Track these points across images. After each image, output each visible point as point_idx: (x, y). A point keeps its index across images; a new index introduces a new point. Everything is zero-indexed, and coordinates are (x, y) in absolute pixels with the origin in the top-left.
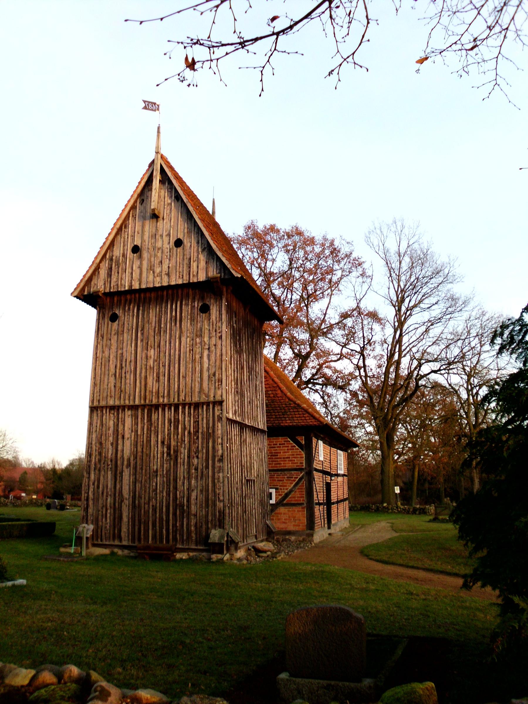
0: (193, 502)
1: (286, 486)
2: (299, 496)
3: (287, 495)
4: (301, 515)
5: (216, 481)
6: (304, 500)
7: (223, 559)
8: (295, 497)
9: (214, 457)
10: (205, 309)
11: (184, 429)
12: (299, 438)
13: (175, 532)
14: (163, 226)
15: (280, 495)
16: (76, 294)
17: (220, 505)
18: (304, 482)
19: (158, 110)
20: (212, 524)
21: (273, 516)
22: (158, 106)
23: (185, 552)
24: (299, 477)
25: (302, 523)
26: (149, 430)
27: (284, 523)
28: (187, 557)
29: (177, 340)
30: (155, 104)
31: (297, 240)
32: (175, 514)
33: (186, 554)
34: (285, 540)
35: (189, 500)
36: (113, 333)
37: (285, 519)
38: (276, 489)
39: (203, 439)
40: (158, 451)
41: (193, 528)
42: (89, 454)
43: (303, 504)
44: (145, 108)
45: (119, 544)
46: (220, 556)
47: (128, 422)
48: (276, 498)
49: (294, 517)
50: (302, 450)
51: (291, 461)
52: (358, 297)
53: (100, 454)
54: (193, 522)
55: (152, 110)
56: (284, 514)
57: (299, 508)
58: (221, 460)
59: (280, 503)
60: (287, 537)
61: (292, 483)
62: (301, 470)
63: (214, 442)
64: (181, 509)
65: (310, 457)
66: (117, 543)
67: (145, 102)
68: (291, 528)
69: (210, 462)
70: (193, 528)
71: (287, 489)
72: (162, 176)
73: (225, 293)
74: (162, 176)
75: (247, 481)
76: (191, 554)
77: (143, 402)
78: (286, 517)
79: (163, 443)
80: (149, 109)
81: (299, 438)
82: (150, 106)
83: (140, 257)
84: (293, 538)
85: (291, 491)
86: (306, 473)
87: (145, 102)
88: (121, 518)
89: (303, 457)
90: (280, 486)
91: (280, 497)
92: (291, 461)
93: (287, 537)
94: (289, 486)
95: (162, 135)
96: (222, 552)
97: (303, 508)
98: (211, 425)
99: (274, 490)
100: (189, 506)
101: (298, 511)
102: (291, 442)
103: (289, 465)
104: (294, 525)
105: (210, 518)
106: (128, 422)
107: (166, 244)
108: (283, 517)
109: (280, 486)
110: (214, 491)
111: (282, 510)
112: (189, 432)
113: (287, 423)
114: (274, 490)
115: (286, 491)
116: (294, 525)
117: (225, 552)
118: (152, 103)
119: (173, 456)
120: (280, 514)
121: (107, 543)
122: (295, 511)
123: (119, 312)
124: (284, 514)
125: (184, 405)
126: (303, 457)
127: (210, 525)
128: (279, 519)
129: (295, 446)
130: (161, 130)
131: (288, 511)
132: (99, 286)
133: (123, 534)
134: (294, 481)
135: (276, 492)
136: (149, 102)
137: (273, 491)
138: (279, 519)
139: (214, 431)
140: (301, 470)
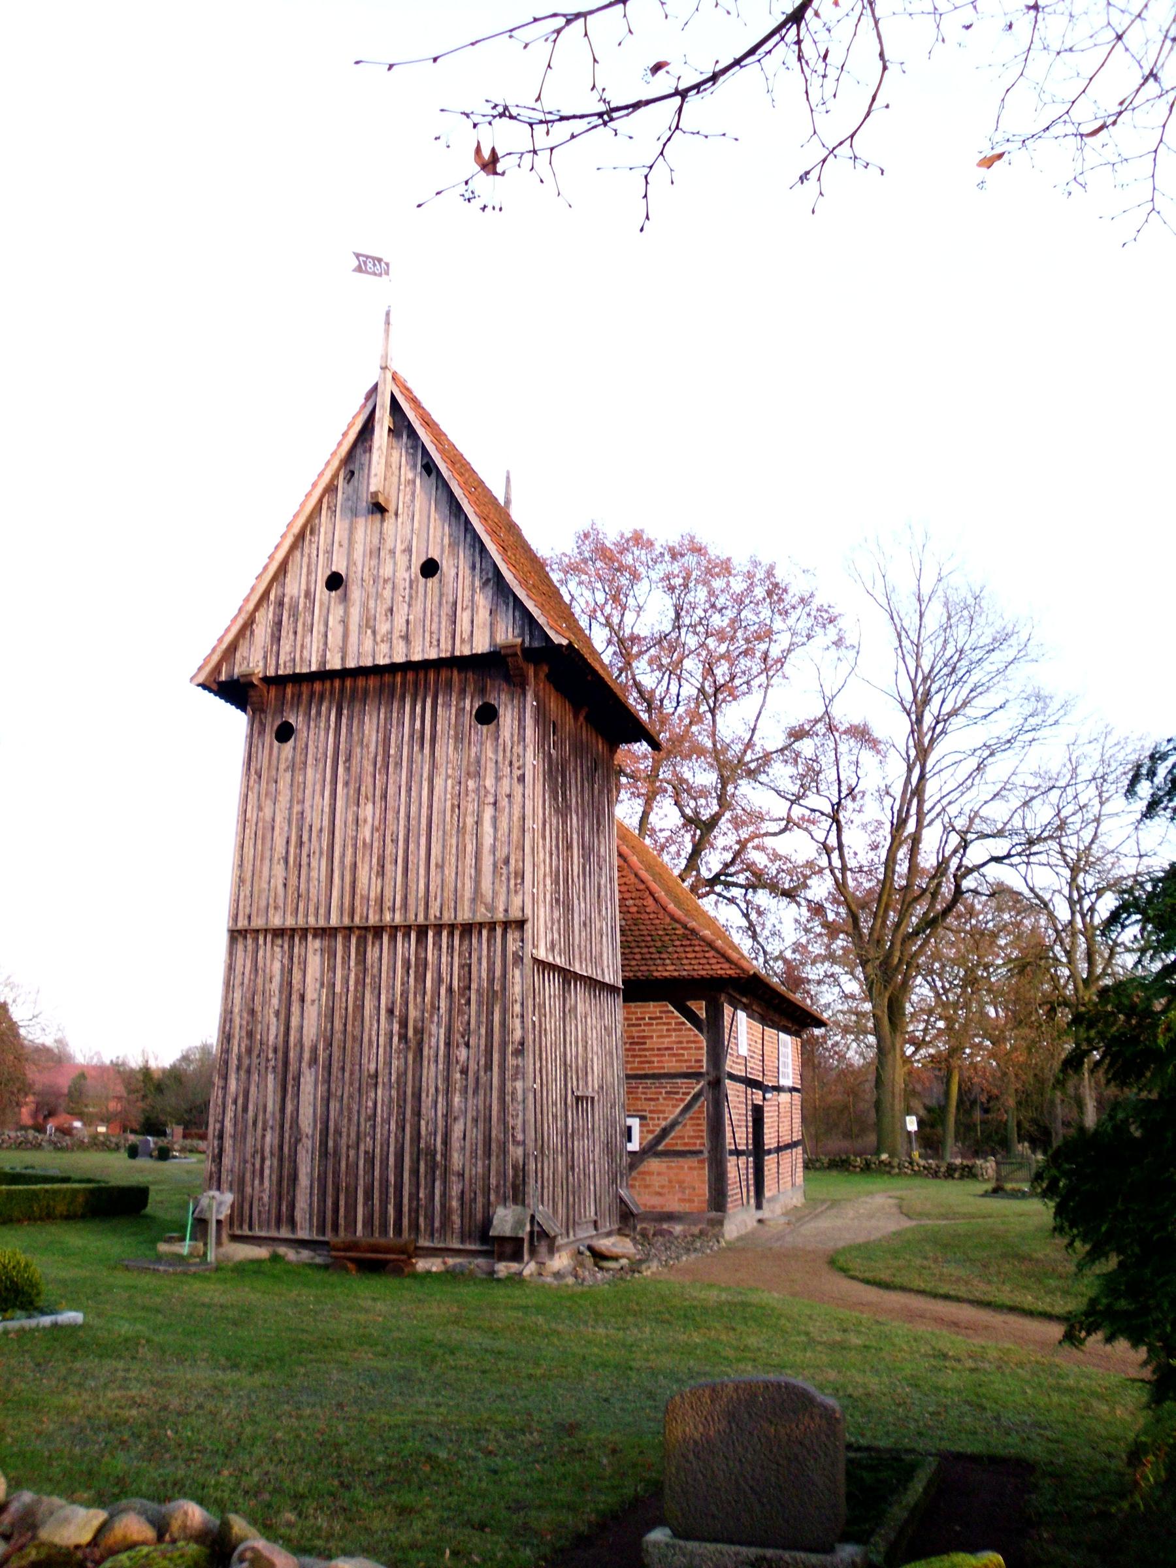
0: (456, 1144)
1: (663, 1112)
2: (692, 1133)
3: (665, 1132)
4: (697, 1177)
5: (508, 1098)
6: (703, 1143)
7: (520, 1274)
8: (682, 1138)
9: (504, 1044)
10: (487, 715)
11: (440, 980)
12: (693, 1005)
13: (414, 1212)
14: (395, 529)
15: (649, 1132)
16: (200, 679)
17: (516, 1152)
19: (387, 273)
20: (497, 1193)
21: (635, 1179)
22: (387, 264)
24: (693, 1092)
26: (361, 983)
27: (660, 1194)
28: (442, 1268)
30: (380, 260)
31: (692, 565)
32: (415, 1172)
33: (438, 1261)
34: (659, 1233)
36: (282, 766)
37: (663, 1187)
38: (642, 1118)
39: (479, 1003)
40: (379, 1029)
42: (226, 1037)
43: (701, 1152)
44: (359, 269)
45: (290, 1236)
46: (514, 1266)
47: (314, 963)
48: (641, 1138)
50: (701, 1030)
51: (675, 1055)
52: (828, 694)
53: (250, 1034)
54: (455, 1190)
56: (659, 1174)
57: (692, 1161)
58: (520, 1052)
59: (649, 1150)
60: (665, 1226)
61: (676, 1106)
62: (697, 1076)
63: (504, 1011)
64: (430, 1162)
65: (717, 1051)
66: (284, 1233)
67: (358, 256)
68: (673, 1204)
69: (496, 1056)
70: (455, 1204)
71: (665, 1119)
73: (532, 680)
74: (397, 419)
75: (578, 1098)
76: (451, 1261)
77: (346, 921)
78: (664, 1180)
79: (390, 1012)
80: (366, 272)
81: (693, 1005)
82: (369, 264)
83: (345, 598)
84: (678, 1229)
86: (709, 1083)
87: (358, 256)
88: (294, 1178)
90: (651, 1112)
91: (650, 1137)
92: (675, 1055)
93: (665, 1226)
94: (671, 1112)
96: (517, 1257)
98: (498, 973)
100: (446, 1155)
101: (690, 1168)
102: (677, 1013)
103: (671, 1065)
104: (682, 1200)
105: (493, 1181)
107: (404, 570)
108: (656, 1182)
109: (651, 1112)
112: (450, 990)
113: (667, 970)
114: (637, 1120)
115: (664, 1124)
117: (526, 1257)
118: (374, 258)
119: (412, 1040)
120: (650, 1174)
121: (263, 1234)
122: (682, 1168)
124: (659, 1174)
125: (439, 928)
126: (701, 1048)
127: (492, 1198)
129: (683, 1023)
131: (668, 1168)
132: (254, 662)
133: (298, 1215)
134: (682, 1100)
135: (641, 1125)
136: (367, 257)
137: (635, 1123)
138: (646, 1186)
139: (504, 988)
140: (697, 1076)
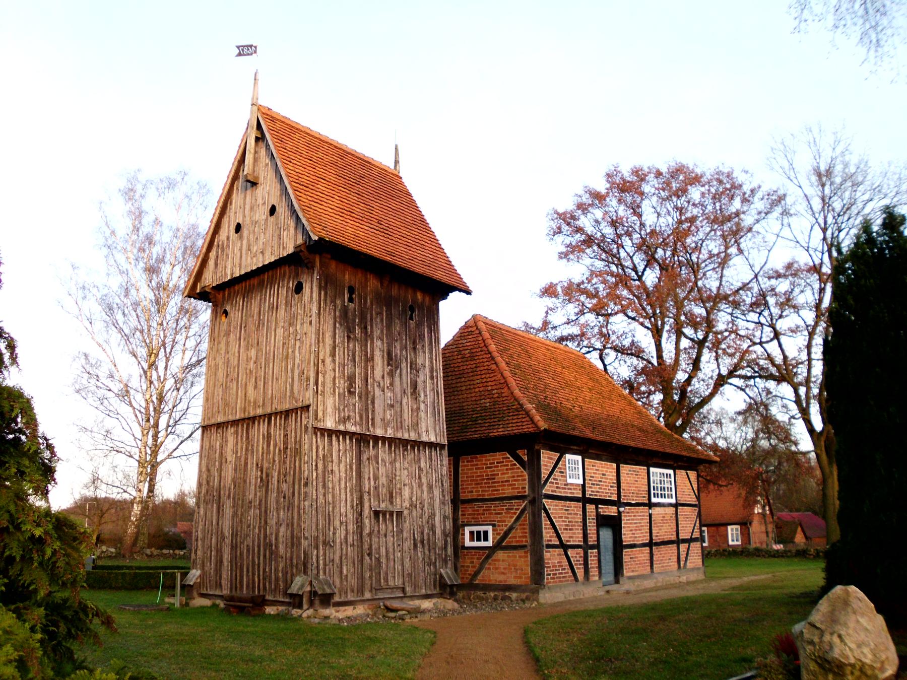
0: (281, 540)
1: (504, 521)
2: (521, 535)
3: (506, 534)
4: (523, 562)
5: (302, 511)
6: (527, 540)
7: (300, 616)
8: (515, 537)
9: (300, 480)
10: (299, 289)
11: (275, 445)
12: (520, 453)
13: (264, 579)
14: (260, 191)
15: (498, 534)
16: (186, 294)
17: (304, 543)
18: (527, 515)
19: (255, 52)
20: (297, 568)
21: (490, 564)
22: (256, 47)
23: (275, 606)
24: (521, 508)
25: (525, 574)
26: (247, 449)
27: (503, 573)
28: (276, 612)
29: (273, 333)
30: (251, 46)
31: (679, 181)
32: (265, 556)
33: (275, 608)
34: (504, 598)
35: (276, 539)
36: (222, 334)
37: (505, 569)
38: (494, 525)
39: (291, 457)
40: (253, 474)
41: (280, 575)
42: (200, 485)
43: (525, 546)
44: (239, 55)
45: (220, 594)
46: (300, 612)
47: (231, 440)
48: (493, 538)
49: (515, 566)
50: (525, 469)
51: (511, 485)
52: (806, 245)
53: (208, 482)
54: (281, 565)
55: (248, 54)
56: (503, 561)
57: (521, 552)
58: (306, 484)
59: (498, 546)
60: (507, 594)
61: (512, 517)
62: (523, 497)
63: (300, 460)
64: (270, 549)
65: (536, 481)
66: (218, 593)
67: (238, 47)
68: (512, 581)
69: (297, 487)
70: (280, 575)
71: (506, 526)
72: (268, 130)
73: (318, 264)
74: (268, 130)
75: (377, 514)
76: (280, 608)
77: (243, 416)
78: (505, 565)
79: (257, 465)
80: (244, 55)
81: (520, 453)
82: (246, 50)
83: (241, 238)
84: (514, 595)
85: (511, 529)
86: (530, 502)
87: (238, 47)
88: (221, 562)
89: (525, 480)
90: (499, 521)
91: (498, 537)
92: (511, 485)
93: (507, 594)
94: (509, 521)
95: (260, 83)
96: (300, 606)
97: (526, 552)
98: (298, 438)
99: (491, 527)
100: (277, 547)
101: (520, 557)
102: (511, 459)
103: (508, 492)
104: (515, 577)
105: (295, 561)
106: (231, 440)
107: (262, 213)
108: (502, 565)
109: (499, 521)
110: (299, 525)
111: (500, 555)
112: (280, 450)
113: (500, 431)
114: (491, 527)
115: (505, 529)
116: (515, 577)
117: (305, 606)
118: (247, 46)
119: (265, 482)
120: (499, 560)
121: (211, 593)
122: (515, 557)
123: (228, 308)
124: (503, 561)
125: (276, 413)
126: (525, 480)
127: (294, 571)
128: (496, 569)
129: (515, 465)
130: (259, 77)
131: (509, 556)
132: (210, 279)
133: (223, 582)
134: (515, 513)
135: (493, 530)
136: (244, 46)
137: (489, 529)
138: (496, 569)
139: (300, 446)
140: (523, 497)
